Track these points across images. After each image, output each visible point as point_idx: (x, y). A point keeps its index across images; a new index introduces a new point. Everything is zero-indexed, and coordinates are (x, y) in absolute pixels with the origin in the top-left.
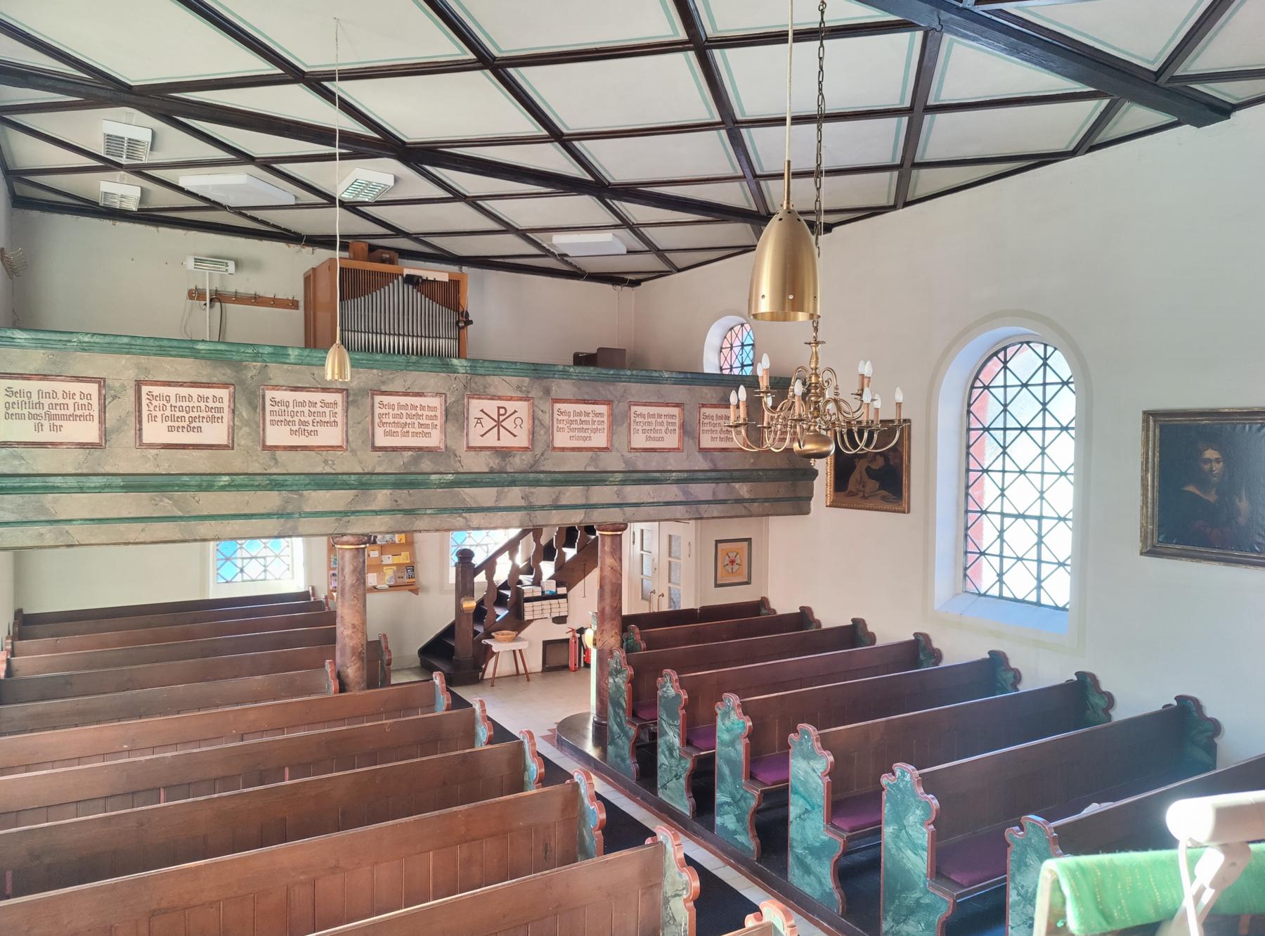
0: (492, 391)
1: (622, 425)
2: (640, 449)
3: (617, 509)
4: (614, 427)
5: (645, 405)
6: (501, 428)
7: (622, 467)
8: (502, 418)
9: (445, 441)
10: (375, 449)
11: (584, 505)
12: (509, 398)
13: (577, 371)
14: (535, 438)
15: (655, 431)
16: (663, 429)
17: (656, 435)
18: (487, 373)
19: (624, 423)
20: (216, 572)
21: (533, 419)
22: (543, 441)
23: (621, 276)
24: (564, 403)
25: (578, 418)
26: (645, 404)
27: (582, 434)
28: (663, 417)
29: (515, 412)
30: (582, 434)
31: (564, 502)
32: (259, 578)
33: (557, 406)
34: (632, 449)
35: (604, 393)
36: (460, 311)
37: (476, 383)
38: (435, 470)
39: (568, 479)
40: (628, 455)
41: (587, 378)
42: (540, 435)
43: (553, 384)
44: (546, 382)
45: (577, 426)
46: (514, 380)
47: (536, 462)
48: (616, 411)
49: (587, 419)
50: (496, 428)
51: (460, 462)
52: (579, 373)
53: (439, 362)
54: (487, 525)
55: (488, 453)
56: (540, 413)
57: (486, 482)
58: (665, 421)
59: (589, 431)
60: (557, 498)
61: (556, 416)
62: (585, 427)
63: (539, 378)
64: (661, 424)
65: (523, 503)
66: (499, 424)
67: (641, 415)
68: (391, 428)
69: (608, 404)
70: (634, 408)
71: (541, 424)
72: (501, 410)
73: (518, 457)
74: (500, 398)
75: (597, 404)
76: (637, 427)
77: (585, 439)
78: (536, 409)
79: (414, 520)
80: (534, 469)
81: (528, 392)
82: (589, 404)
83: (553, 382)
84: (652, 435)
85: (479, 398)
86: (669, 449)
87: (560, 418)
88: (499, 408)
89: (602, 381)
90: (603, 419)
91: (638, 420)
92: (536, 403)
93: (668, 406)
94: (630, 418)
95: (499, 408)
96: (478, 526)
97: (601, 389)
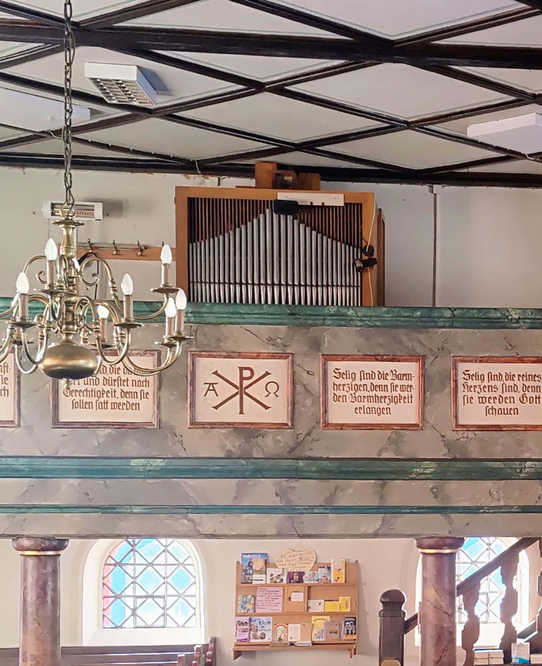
0: (229, 345)
1: (441, 391)
2: (473, 426)
3: (438, 517)
4: (428, 394)
5: (480, 362)
6: (244, 396)
7: (442, 453)
8: (246, 383)
9: (159, 413)
10: (57, 423)
11: (378, 508)
12: (255, 355)
13: (359, 314)
14: (297, 411)
15: (502, 399)
16: (517, 396)
17: (503, 406)
18: (220, 321)
19: (444, 386)
20: (102, 613)
21: (294, 384)
22: (309, 414)
23: (465, 170)
24: (343, 360)
25: (368, 382)
26: (482, 360)
27: (376, 405)
28: (516, 379)
29: (267, 374)
30: (376, 405)
31: (343, 502)
32: (157, 624)
33: (333, 365)
34: (457, 426)
35: (410, 344)
36: (363, 246)
37: (205, 335)
38: (143, 455)
39: (344, 469)
40: (451, 435)
41: (378, 324)
42: (305, 406)
43: (325, 334)
44: (314, 331)
45: (366, 394)
46: (264, 330)
47: (299, 444)
48: (432, 370)
49: (383, 382)
50: (238, 396)
51: (181, 443)
52: (365, 316)
53: (147, 309)
54: (226, 532)
55: (223, 431)
56: (305, 375)
57: (215, 471)
58: (520, 384)
59: (387, 401)
60: (333, 496)
61: (331, 379)
62: (380, 394)
63: (301, 325)
64: (514, 388)
65: (277, 502)
66: (242, 391)
67: (476, 376)
68: (82, 398)
69: (417, 361)
70: (462, 367)
71: (307, 390)
72: (244, 371)
73: (271, 437)
74: (240, 355)
75: (399, 361)
76: (470, 394)
77: (379, 412)
78: (297, 369)
79: (118, 520)
80: (296, 454)
81: (285, 346)
82: (384, 361)
83: (325, 330)
84: (497, 406)
85: (210, 356)
86: (526, 426)
87: (337, 382)
88: (241, 369)
89: (403, 327)
90: (409, 383)
91: (470, 383)
92: (298, 360)
93: (523, 362)
94: (456, 381)
95: (241, 369)
96: (212, 532)
97: (404, 339)
